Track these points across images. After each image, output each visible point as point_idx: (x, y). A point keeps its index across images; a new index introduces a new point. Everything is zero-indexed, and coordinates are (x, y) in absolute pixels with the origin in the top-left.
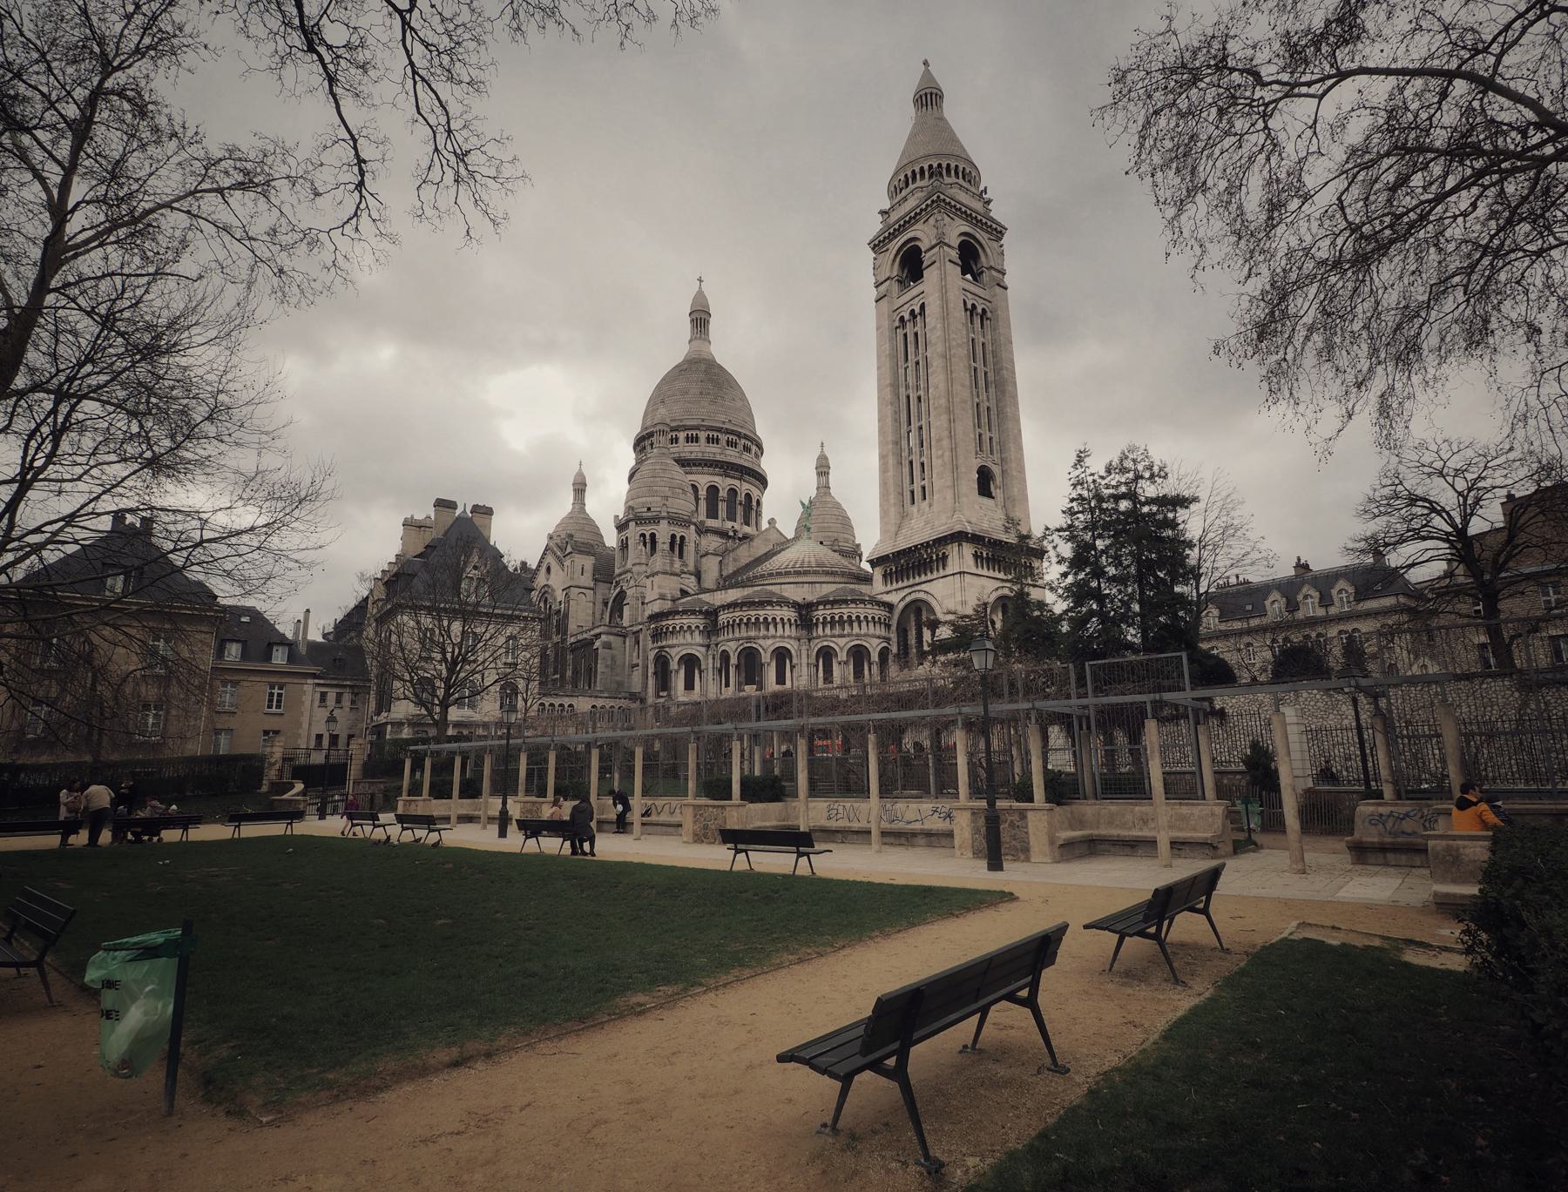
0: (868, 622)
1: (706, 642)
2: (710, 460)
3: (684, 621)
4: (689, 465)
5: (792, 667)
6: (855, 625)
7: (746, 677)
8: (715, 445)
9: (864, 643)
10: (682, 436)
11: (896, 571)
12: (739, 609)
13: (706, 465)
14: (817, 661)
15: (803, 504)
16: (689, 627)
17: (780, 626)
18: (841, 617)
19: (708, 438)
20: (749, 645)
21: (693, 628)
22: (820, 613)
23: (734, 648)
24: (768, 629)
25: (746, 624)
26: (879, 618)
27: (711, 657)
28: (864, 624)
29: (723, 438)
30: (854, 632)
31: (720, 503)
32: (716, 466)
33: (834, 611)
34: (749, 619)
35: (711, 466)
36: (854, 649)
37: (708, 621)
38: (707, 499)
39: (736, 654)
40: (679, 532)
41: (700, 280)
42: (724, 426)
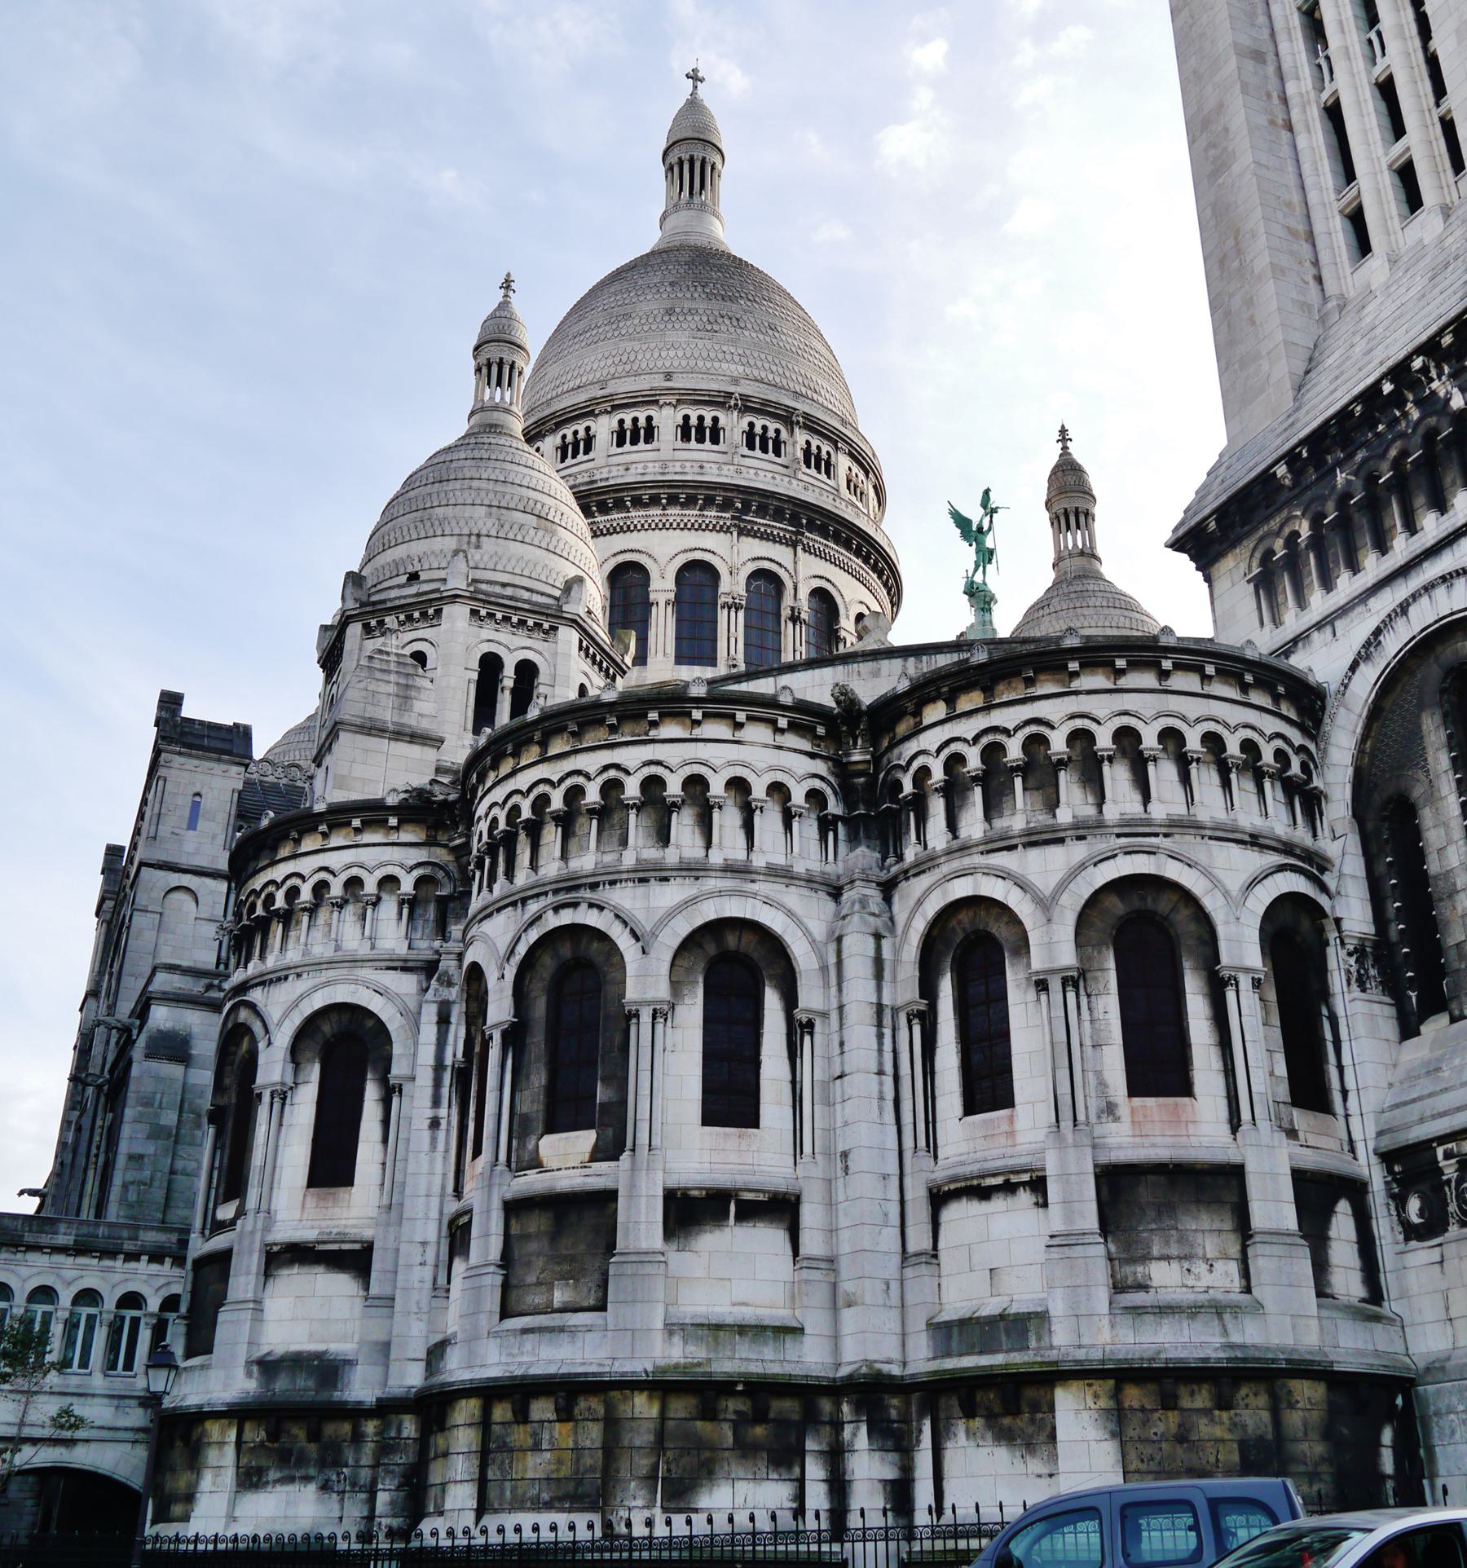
0: (1184, 763)
1: (426, 947)
2: (684, 484)
3: (333, 860)
4: (620, 505)
5: (798, 1030)
6: (1117, 777)
7: (552, 1091)
8: (708, 445)
9: (1173, 871)
10: (603, 428)
11: (1317, 542)
12: (532, 754)
13: (673, 500)
14: (928, 990)
15: (962, 522)
16: (354, 883)
17: (727, 820)
18: (1037, 743)
19: (685, 431)
20: (567, 917)
21: (370, 886)
22: (930, 740)
23: (503, 945)
24: (663, 837)
25: (567, 822)
26: (1248, 746)
27: (430, 1014)
28: (1163, 775)
29: (734, 425)
30: (1111, 813)
31: (722, 615)
32: (709, 502)
33: (999, 718)
34: (574, 794)
35: (690, 502)
36: (1116, 906)
37: (441, 855)
38: (678, 602)
39: (511, 972)
40: (513, 648)
41: (694, 77)
42: (737, 390)
